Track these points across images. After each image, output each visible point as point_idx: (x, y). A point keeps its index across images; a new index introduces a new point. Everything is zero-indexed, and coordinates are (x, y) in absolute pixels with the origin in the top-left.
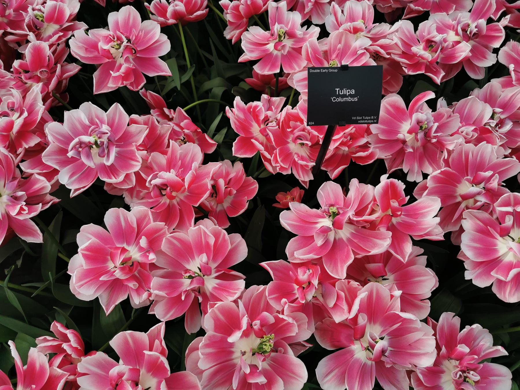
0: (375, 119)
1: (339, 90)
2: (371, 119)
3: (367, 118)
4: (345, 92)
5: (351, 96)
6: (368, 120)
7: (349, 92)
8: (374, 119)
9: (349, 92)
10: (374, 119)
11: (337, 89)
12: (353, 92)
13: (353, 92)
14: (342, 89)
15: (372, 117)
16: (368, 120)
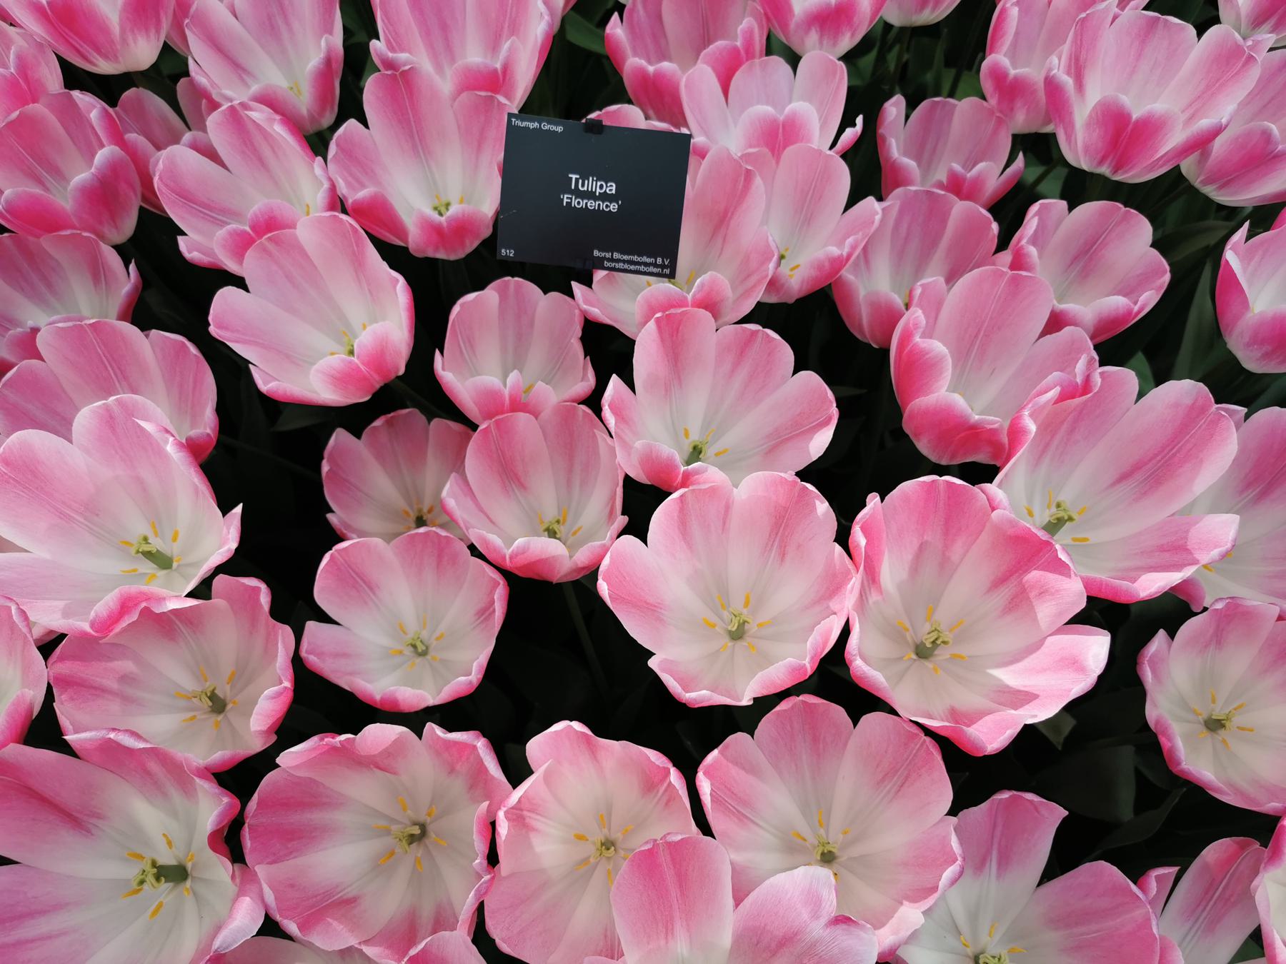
0: (666, 267)
1: (577, 180)
2: (655, 265)
3: (645, 259)
4: (593, 185)
5: (605, 197)
6: (646, 264)
7: (601, 187)
8: (663, 266)
9: (601, 187)
10: (663, 266)
11: (574, 177)
12: (612, 188)
13: (612, 188)
14: (584, 177)
15: (659, 261)
16: (646, 264)
